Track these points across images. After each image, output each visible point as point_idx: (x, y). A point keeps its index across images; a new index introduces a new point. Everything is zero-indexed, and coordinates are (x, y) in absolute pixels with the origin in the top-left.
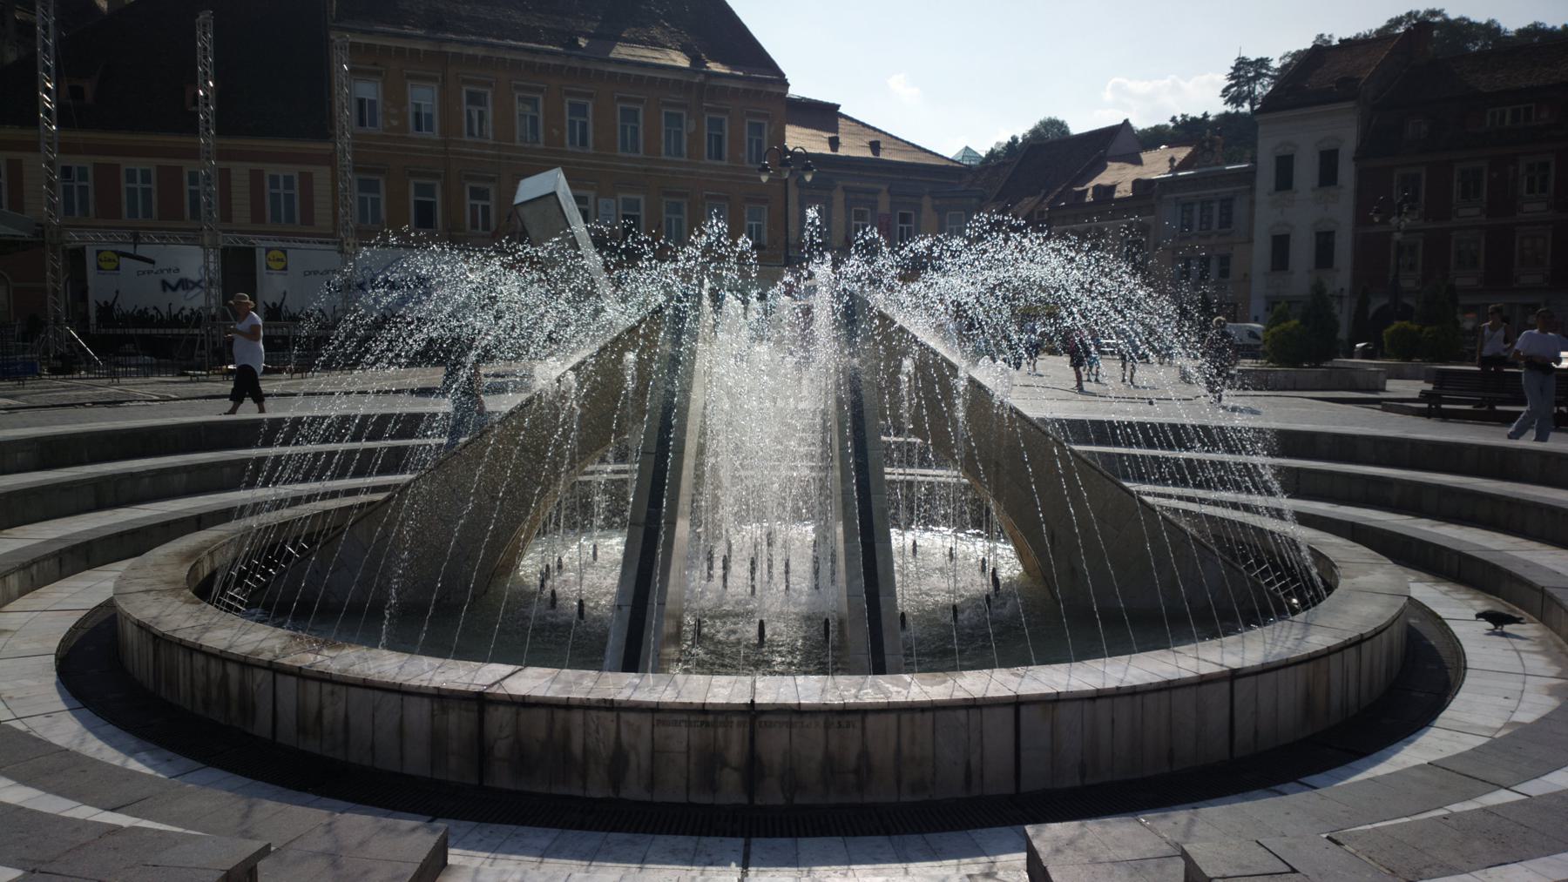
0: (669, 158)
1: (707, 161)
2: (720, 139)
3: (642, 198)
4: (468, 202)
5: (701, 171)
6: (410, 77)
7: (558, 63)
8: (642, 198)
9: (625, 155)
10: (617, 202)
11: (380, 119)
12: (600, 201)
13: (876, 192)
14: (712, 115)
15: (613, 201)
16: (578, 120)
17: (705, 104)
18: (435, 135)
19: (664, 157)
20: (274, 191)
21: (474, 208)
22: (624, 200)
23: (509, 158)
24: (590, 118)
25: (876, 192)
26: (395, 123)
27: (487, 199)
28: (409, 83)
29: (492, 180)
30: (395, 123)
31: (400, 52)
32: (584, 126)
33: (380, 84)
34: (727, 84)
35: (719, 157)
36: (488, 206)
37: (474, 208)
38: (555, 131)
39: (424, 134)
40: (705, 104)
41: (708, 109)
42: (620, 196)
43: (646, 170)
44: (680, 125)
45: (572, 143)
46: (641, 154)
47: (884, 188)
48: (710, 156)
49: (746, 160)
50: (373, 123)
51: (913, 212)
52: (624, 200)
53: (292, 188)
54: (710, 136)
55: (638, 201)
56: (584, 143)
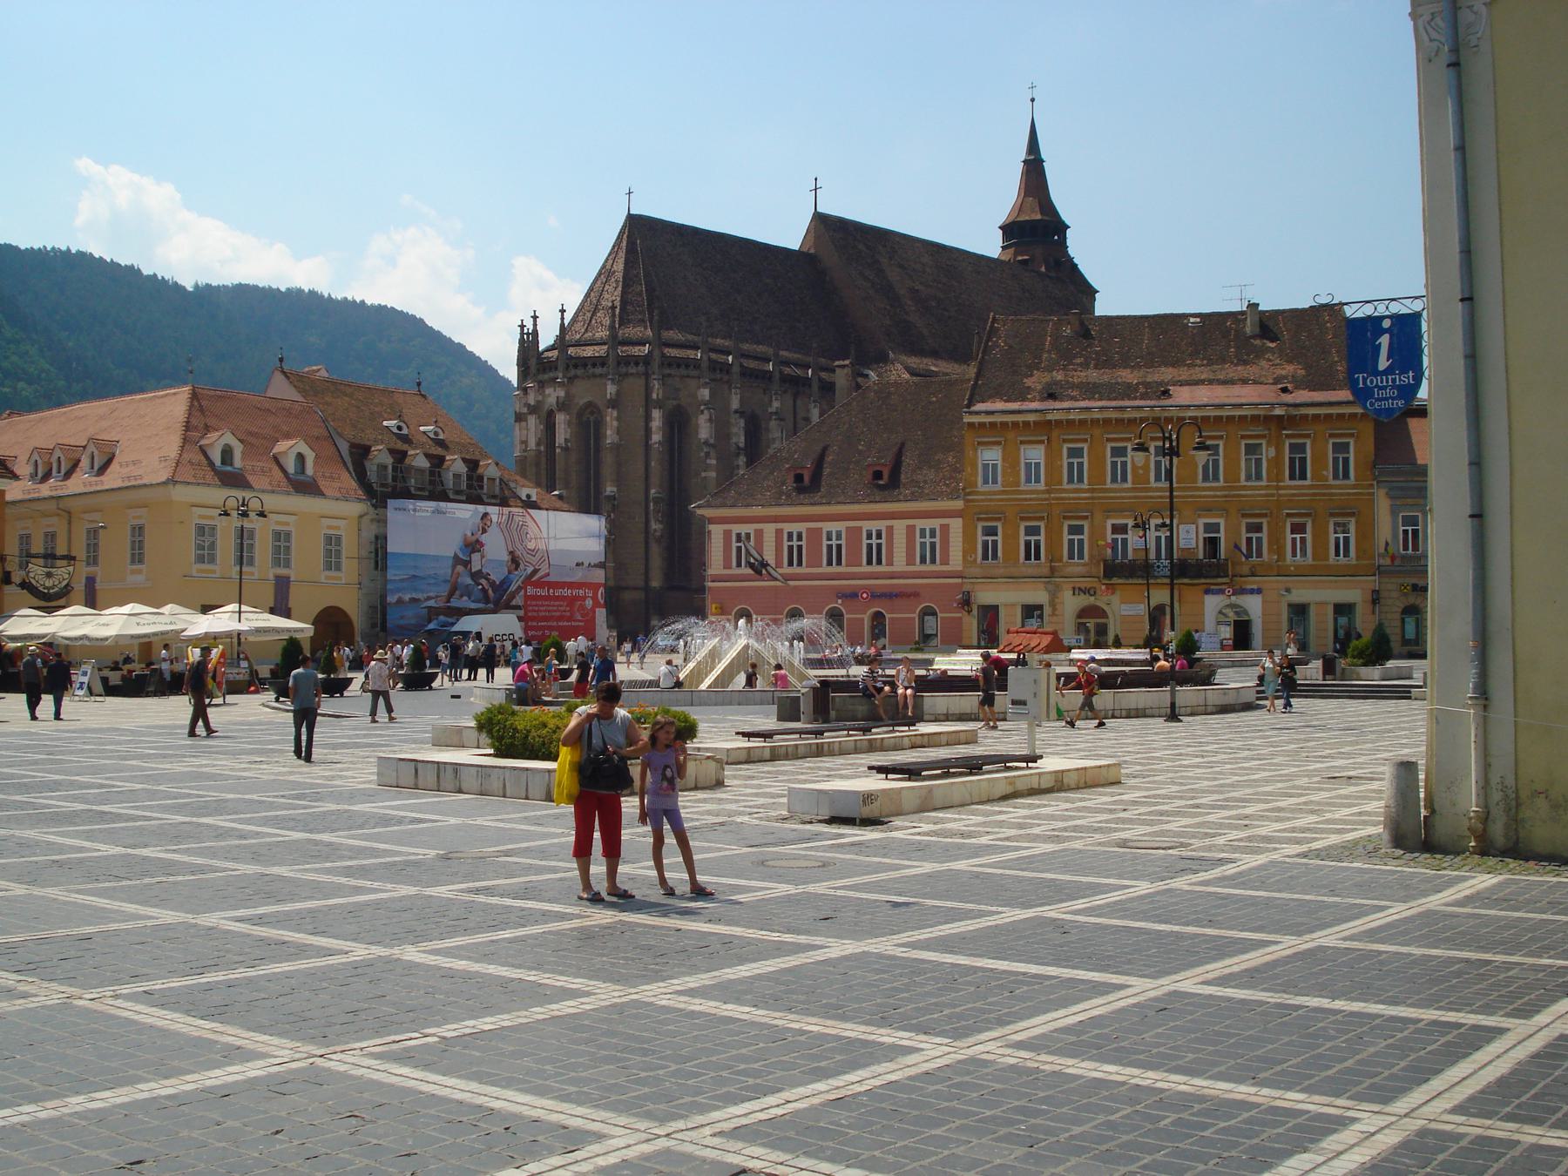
0: (1249, 484)
1: (1288, 482)
2: (1303, 461)
3: (1222, 521)
6: (1022, 442)
8: (1222, 521)
10: (1197, 528)
15: (1194, 526)
18: (1042, 486)
19: (1243, 483)
29: (1086, 518)
34: (1306, 412)
39: (1033, 486)
42: (1201, 522)
43: (1226, 496)
46: (1221, 483)
48: (1292, 477)
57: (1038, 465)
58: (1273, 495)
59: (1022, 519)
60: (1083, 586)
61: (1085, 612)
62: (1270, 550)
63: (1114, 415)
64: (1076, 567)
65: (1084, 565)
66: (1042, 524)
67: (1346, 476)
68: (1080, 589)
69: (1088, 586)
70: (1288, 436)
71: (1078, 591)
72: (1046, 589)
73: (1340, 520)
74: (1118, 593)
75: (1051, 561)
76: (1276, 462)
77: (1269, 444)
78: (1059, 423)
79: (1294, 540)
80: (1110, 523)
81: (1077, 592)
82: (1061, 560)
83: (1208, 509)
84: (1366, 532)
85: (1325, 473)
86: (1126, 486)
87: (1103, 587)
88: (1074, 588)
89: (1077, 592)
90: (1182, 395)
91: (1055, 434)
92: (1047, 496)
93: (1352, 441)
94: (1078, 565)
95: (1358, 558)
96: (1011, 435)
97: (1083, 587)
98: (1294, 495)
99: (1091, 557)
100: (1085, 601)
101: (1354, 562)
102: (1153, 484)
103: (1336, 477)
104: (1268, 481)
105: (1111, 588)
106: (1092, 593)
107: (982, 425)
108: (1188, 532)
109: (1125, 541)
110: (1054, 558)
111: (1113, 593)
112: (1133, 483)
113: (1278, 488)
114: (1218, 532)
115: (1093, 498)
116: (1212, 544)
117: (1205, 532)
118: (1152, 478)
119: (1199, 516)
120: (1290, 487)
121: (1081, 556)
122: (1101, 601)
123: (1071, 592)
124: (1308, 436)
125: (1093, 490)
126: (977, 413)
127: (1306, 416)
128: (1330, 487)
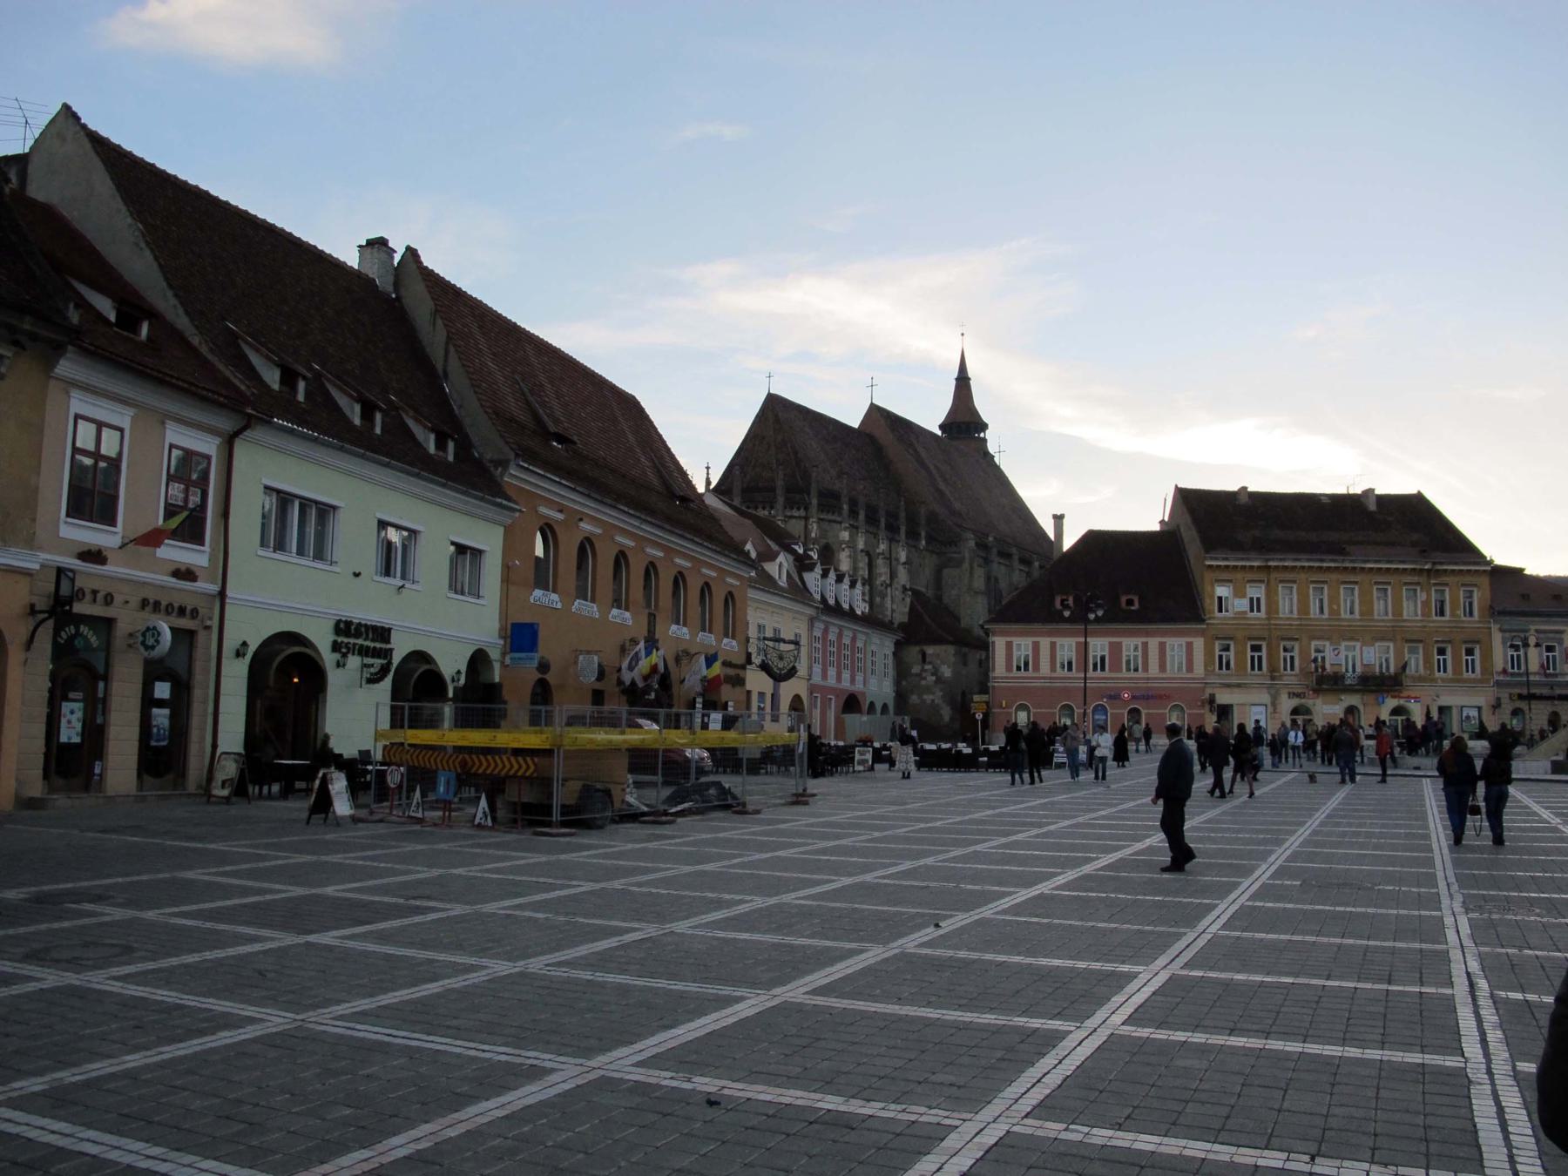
1: (1435, 618)
4: (1282, 654)
5: (1432, 625)
18: (1263, 614)
28: (1248, 585)
29: (1297, 639)
31: (1243, 567)
35: (1442, 613)
37: (1253, 658)
41: (1435, 584)
42: (1377, 644)
46: (1390, 617)
54: (1436, 601)
57: (1258, 599)
58: (1425, 627)
60: (1296, 691)
61: (1295, 711)
62: (1425, 668)
63: (1316, 564)
64: (1290, 678)
67: (1471, 614)
68: (1294, 694)
69: (1300, 691)
70: (1435, 584)
71: (1292, 695)
72: (1269, 693)
73: (1469, 646)
76: (1426, 604)
77: (1422, 591)
78: (1276, 567)
82: (1279, 672)
84: (1487, 656)
85: (1458, 612)
88: (1289, 693)
92: (1267, 622)
93: (1475, 589)
95: (1482, 674)
96: (1239, 576)
100: (1295, 702)
101: (1479, 676)
102: (1343, 616)
103: (1465, 615)
108: (1369, 653)
110: (1273, 669)
113: (1429, 622)
115: (1301, 625)
120: (1434, 621)
122: (1308, 702)
124: (1447, 585)
125: (1300, 619)
127: (1446, 571)
128: (1463, 622)
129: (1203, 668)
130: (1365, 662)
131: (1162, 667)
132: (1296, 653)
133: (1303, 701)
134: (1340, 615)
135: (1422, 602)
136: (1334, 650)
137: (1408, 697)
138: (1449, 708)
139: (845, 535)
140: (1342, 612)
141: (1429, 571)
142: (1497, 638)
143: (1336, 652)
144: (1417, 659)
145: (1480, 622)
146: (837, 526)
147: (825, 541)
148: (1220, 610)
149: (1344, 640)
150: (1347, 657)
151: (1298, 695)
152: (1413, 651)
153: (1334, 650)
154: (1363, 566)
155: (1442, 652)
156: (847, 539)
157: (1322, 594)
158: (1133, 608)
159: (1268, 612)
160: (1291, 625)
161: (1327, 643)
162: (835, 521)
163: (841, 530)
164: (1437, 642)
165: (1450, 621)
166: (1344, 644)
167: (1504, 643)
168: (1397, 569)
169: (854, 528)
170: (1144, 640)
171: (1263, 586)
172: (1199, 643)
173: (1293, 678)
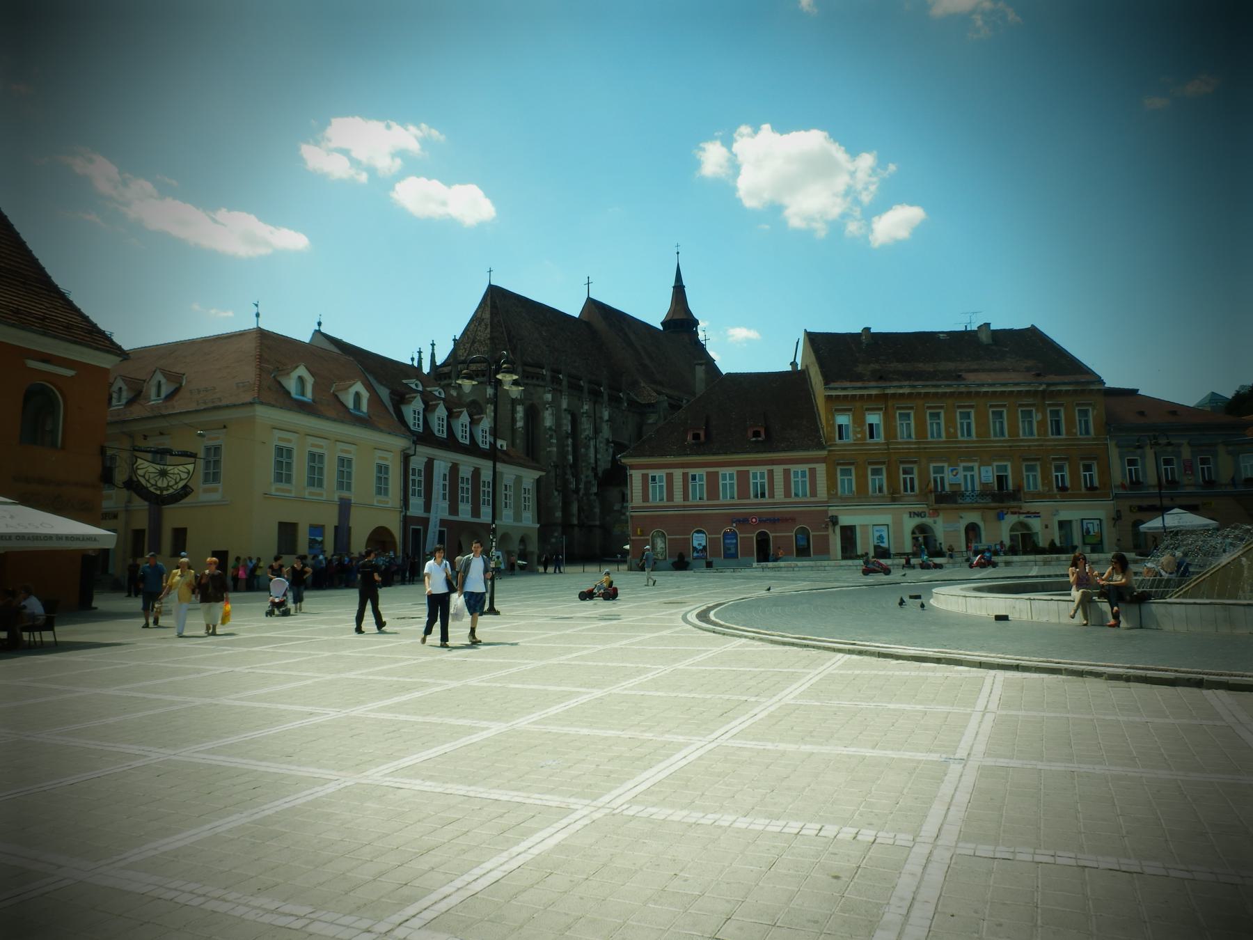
0: (1025, 438)
1: (1052, 437)
2: (1058, 423)
3: (1009, 464)
4: (902, 476)
7: (952, 390)
8: (1009, 464)
9: (997, 438)
10: (993, 469)
11: (851, 435)
12: (982, 468)
13: (1180, 445)
14: (1052, 408)
15: (990, 468)
16: (965, 422)
17: (1047, 402)
19: (1022, 438)
20: (804, 479)
21: (905, 480)
22: (997, 466)
23: (925, 448)
24: (973, 419)
25: (1180, 445)
26: (859, 436)
27: (912, 473)
28: (867, 413)
29: (915, 462)
30: (859, 436)
31: (862, 397)
32: (969, 425)
33: (851, 416)
35: (1058, 433)
36: (913, 478)
38: (952, 430)
40: (1047, 402)
42: (995, 464)
43: (1010, 447)
44: (1031, 417)
45: (963, 435)
46: (1007, 437)
47: (1185, 442)
48: (1052, 434)
49: (1079, 433)
50: (848, 437)
51: (1210, 457)
52: (997, 466)
53: (733, 479)
54: (1051, 421)
55: (1006, 466)
56: (969, 434)
58: (1042, 446)
59: (870, 463)
62: (1043, 484)
65: (916, 496)
66: (884, 468)
68: (914, 513)
69: (920, 510)
73: (1087, 462)
74: (941, 514)
75: (893, 494)
76: (1042, 424)
77: (1037, 411)
78: (894, 395)
79: (1085, 476)
80: (932, 465)
81: (912, 515)
82: (899, 493)
83: (1000, 455)
84: (1105, 471)
86: (941, 440)
87: (931, 511)
88: (910, 513)
89: (912, 515)
90: (971, 378)
91: (890, 403)
92: (886, 447)
94: (912, 496)
96: (858, 404)
97: (916, 511)
98: (1055, 445)
99: (921, 490)
100: (917, 521)
102: (960, 438)
104: (1039, 435)
105: (936, 512)
106: (923, 515)
107: (838, 397)
108: (987, 472)
109: (942, 479)
111: (938, 516)
112: (946, 438)
113: (1048, 440)
114: (1006, 471)
115: (919, 448)
116: (1001, 480)
117: (997, 472)
118: (959, 435)
119: (995, 460)
121: (912, 489)
122: (928, 520)
123: (909, 515)
126: (836, 389)
128: (1078, 439)
129: (826, 492)
130: (983, 481)
131: (787, 493)
132: (915, 475)
133: (924, 520)
134: (957, 438)
135: (1038, 422)
136: (952, 471)
137: (1028, 513)
138: (1070, 522)
139: (549, 397)
140: (959, 435)
141: (1043, 392)
142: (1114, 453)
143: (954, 473)
144: (1035, 477)
145: (1094, 439)
146: (539, 389)
147: (531, 402)
148: (841, 437)
149: (962, 461)
150: (965, 477)
151: (918, 515)
152: (1030, 469)
153: (952, 471)
154: (978, 390)
155: (1088, 468)
156: (550, 400)
157: (939, 419)
158: (760, 439)
159: (886, 438)
160: (911, 449)
161: (946, 465)
162: (538, 386)
163: (545, 393)
164: (1054, 459)
165: (1066, 439)
166: (962, 465)
167: (1121, 457)
168: (1012, 392)
169: (557, 392)
170: (770, 467)
171: (881, 413)
172: (821, 469)
173: (913, 498)
